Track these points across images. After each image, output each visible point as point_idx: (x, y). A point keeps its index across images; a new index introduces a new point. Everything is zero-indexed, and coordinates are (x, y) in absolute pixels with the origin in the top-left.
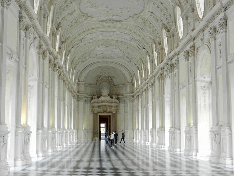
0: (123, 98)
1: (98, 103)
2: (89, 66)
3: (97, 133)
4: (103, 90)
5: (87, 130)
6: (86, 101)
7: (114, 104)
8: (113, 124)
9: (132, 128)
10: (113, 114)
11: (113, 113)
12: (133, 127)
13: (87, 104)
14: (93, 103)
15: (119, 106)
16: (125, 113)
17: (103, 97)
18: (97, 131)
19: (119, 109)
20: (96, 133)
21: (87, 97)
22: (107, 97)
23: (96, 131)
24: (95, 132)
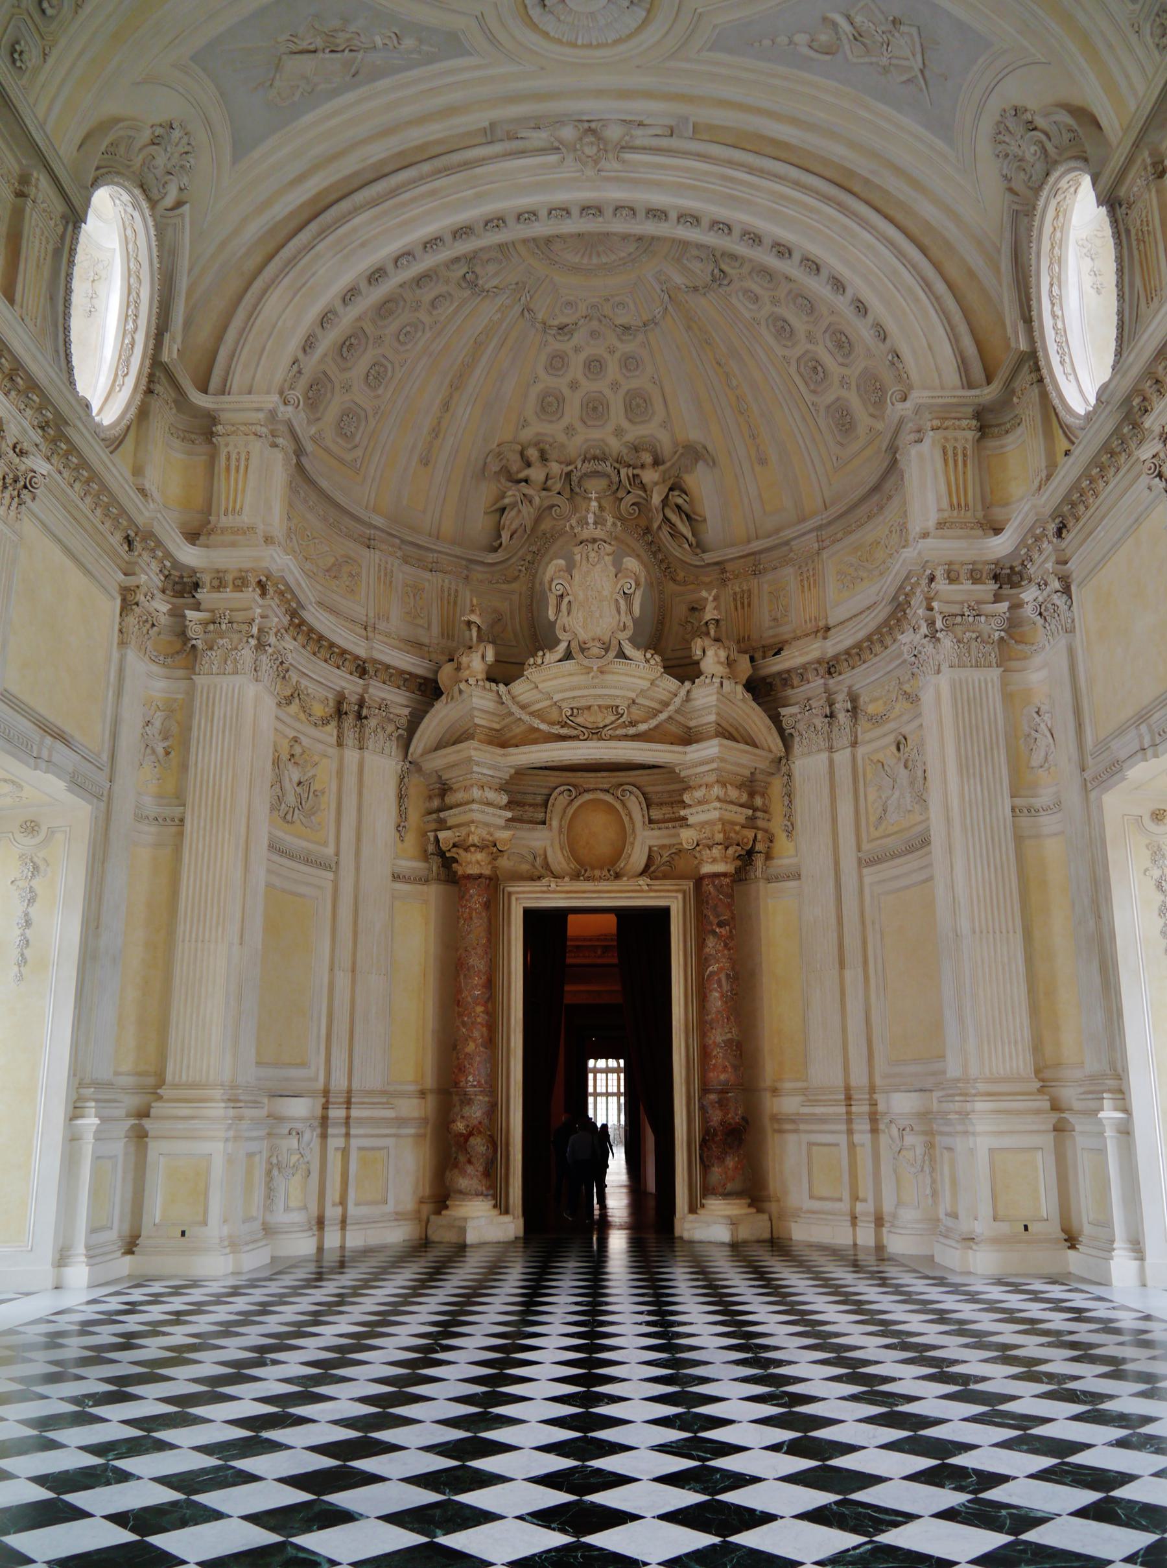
0: (831, 667)
1: (501, 740)
2: (374, 203)
3: (493, 1143)
4: (570, 568)
5: (348, 1104)
6: (340, 713)
7: (710, 749)
8: (701, 1025)
9: (1020, 1063)
10: (699, 880)
11: (707, 869)
12: (1037, 1047)
13: (351, 755)
14: (439, 747)
15: (777, 785)
16: (866, 862)
17: (568, 656)
18: (494, 1110)
19: (777, 825)
20: (478, 1145)
21: (362, 669)
22: (622, 655)
23: (476, 1112)
24: (460, 1126)
